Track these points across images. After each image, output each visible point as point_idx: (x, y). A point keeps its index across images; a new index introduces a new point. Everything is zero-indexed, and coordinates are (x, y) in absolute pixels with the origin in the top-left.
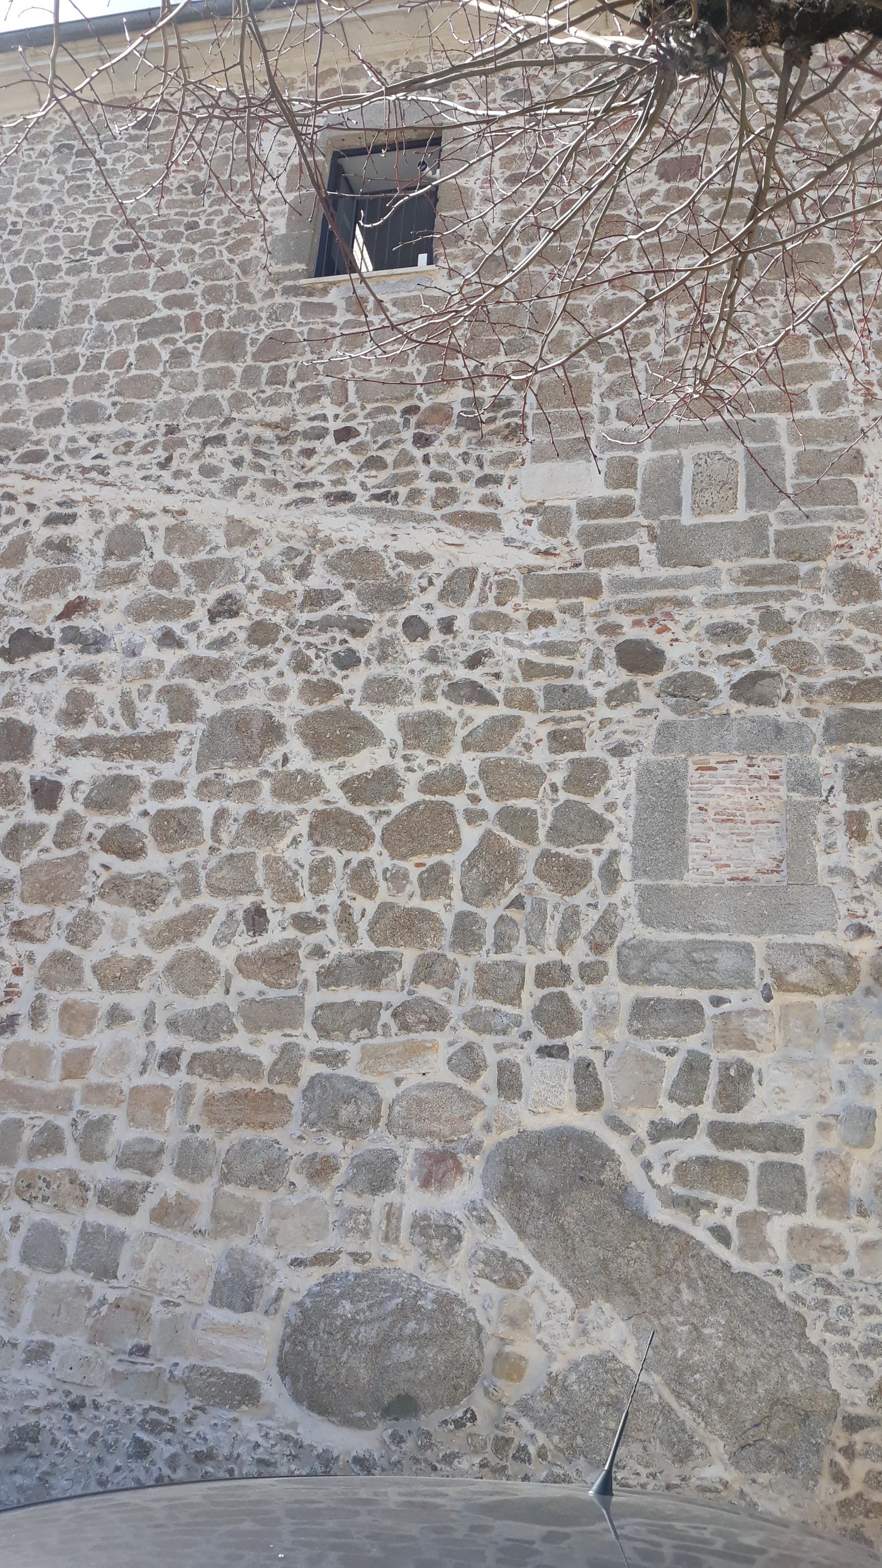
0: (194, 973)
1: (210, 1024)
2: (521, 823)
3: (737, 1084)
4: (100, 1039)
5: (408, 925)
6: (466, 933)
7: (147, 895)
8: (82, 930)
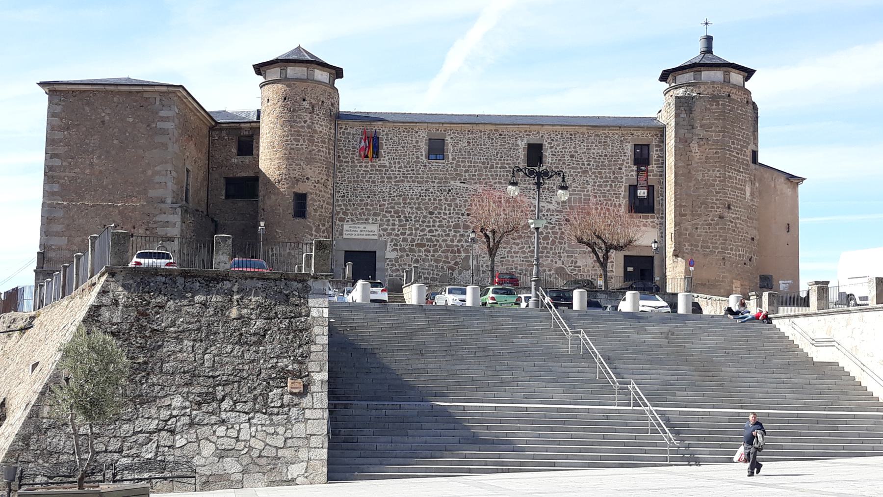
0: (524, 252)
1: (526, 257)
2: (556, 238)
3: (576, 262)
4: (515, 259)
5: (546, 248)
6: (551, 249)
7: (518, 245)
8: (511, 248)
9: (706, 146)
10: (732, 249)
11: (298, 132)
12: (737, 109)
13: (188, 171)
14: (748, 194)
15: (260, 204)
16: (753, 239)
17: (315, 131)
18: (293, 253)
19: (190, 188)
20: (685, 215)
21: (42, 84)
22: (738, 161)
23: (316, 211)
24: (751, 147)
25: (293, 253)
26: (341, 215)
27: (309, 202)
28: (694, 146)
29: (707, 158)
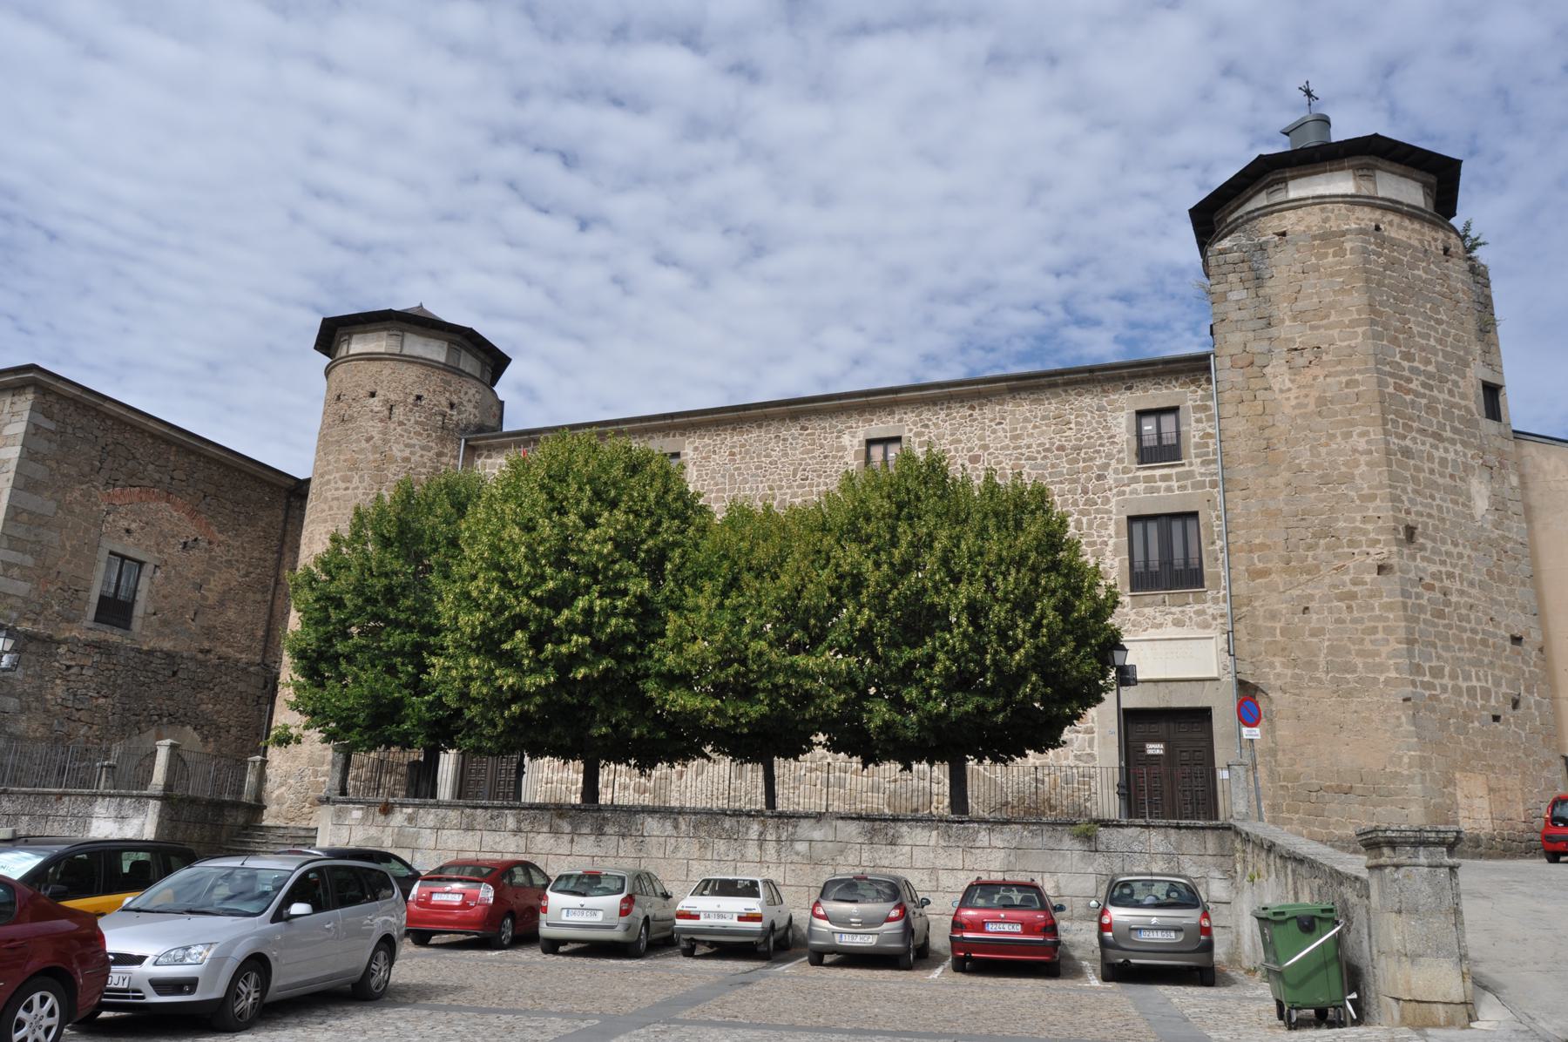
9: (1315, 370)
12: (1412, 266)
14: (1481, 504)
16: (1516, 640)
22: (1430, 408)
24: (1478, 372)
28: (1279, 376)
29: (1321, 401)
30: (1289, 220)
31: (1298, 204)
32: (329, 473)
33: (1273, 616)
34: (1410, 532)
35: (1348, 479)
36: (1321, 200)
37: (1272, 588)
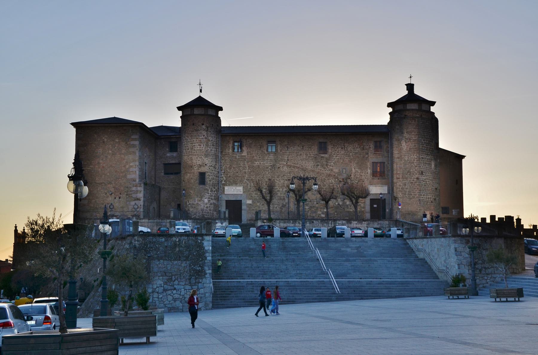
10: (424, 195)
11: (200, 141)
13: (146, 163)
15: (182, 178)
16: (436, 189)
17: (209, 140)
18: (199, 203)
19: (147, 172)
20: (399, 178)
21: (73, 124)
23: (210, 181)
25: (199, 203)
26: (223, 182)
27: (207, 176)
29: (410, 149)
30: (407, 113)
31: (409, 110)
32: (195, 143)
33: (400, 186)
34: (422, 173)
35: (413, 163)
36: (413, 110)
37: (400, 181)
